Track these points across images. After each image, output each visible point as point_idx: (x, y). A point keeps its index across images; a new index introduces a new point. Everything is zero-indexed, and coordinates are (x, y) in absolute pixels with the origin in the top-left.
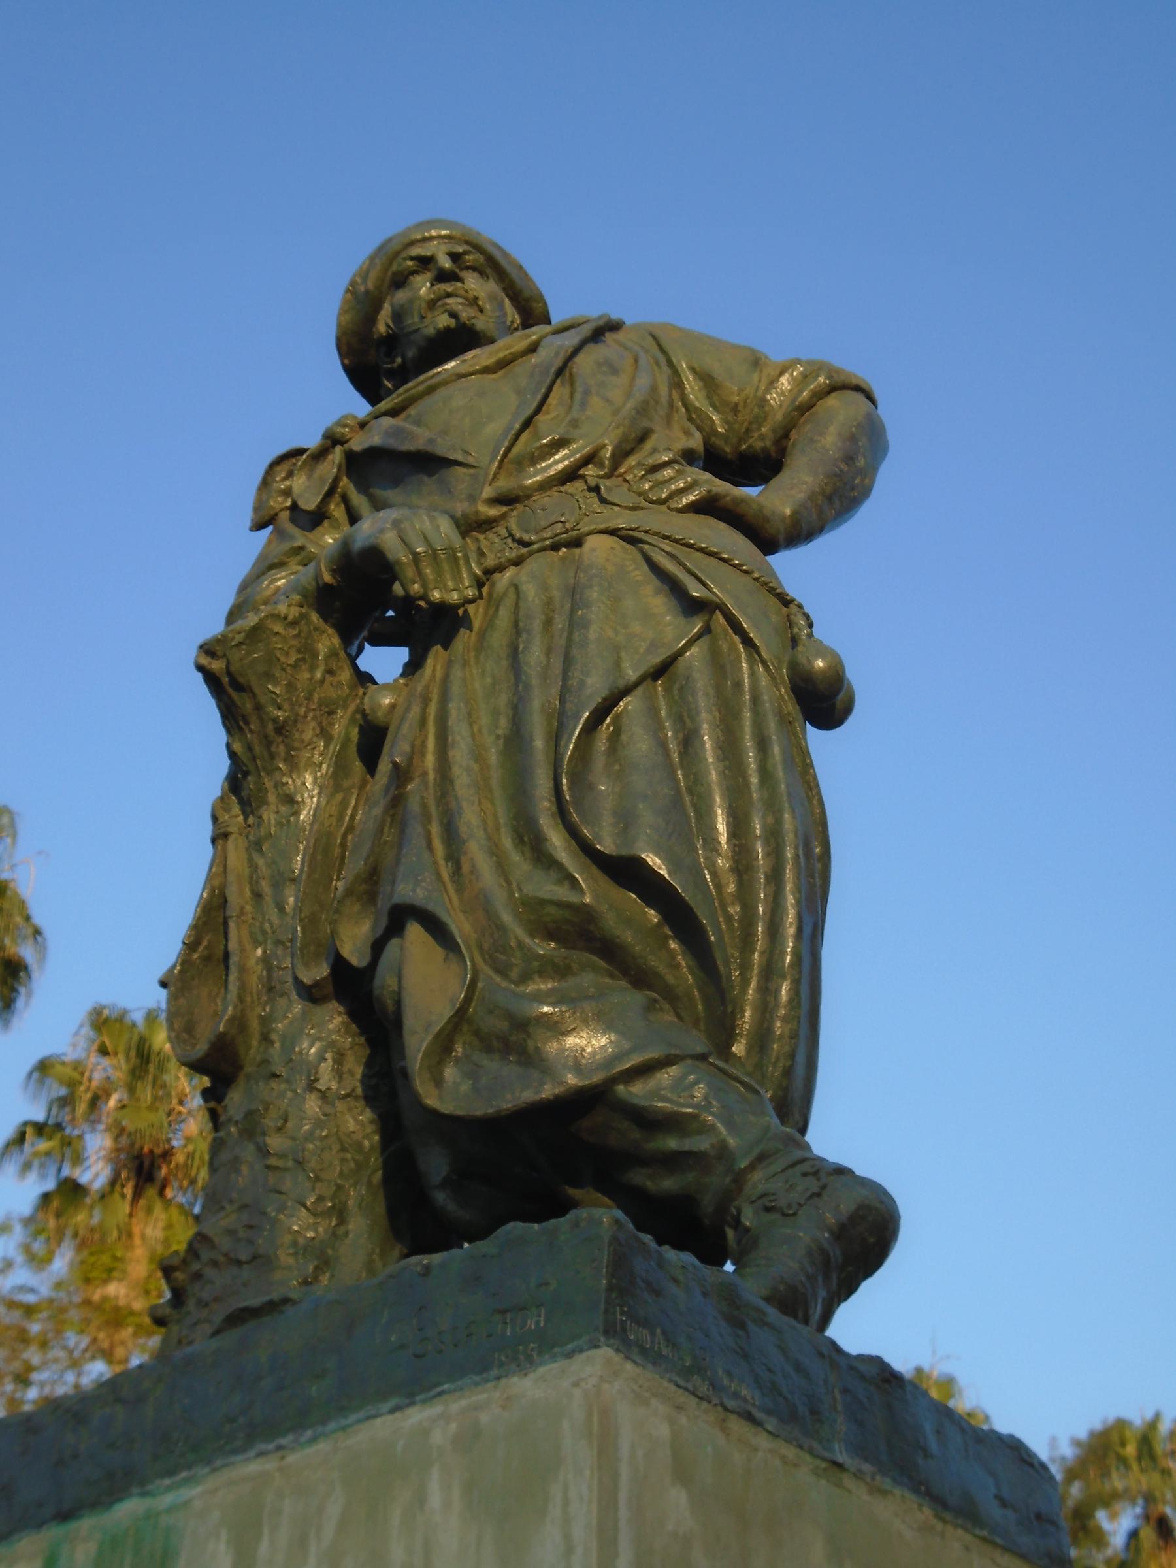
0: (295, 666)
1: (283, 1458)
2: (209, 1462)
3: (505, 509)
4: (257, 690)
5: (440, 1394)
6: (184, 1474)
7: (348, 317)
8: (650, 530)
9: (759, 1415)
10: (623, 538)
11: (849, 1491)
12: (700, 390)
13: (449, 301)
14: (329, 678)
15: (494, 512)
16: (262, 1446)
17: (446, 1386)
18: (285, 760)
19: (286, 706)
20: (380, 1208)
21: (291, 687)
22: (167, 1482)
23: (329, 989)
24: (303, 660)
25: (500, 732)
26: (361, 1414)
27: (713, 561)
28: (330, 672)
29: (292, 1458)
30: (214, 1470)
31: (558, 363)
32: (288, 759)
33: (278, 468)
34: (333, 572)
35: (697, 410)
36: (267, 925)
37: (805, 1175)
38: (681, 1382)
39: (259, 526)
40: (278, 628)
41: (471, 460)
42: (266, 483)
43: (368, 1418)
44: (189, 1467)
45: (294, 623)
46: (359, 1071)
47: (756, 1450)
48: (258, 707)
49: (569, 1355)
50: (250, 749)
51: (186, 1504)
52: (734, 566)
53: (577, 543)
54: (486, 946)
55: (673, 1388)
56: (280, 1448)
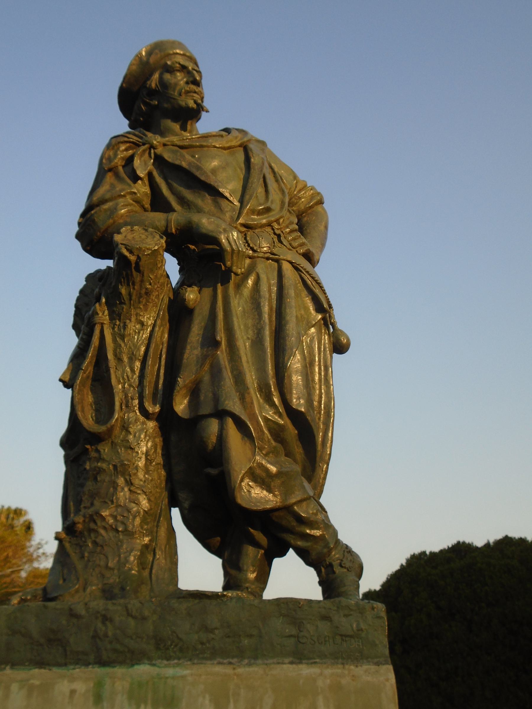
1: (234, 669)
2: (190, 660)
4: (145, 274)
6: (176, 661)
8: (303, 267)
10: (293, 266)
13: (195, 95)
17: (318, 660)
18: (144, 305)
22: (165, 662)
23: (155, 416)
26: (275, 660)
29: (240, 670)
30: (194, 664)
34: (177, 229)
36: (125, 377)
43: (279, 663)
44: (179, 659)
46: (160, 452)
48: (142, 281)
50: (130, 295)
51: (183, 677)
56: (230, 663)
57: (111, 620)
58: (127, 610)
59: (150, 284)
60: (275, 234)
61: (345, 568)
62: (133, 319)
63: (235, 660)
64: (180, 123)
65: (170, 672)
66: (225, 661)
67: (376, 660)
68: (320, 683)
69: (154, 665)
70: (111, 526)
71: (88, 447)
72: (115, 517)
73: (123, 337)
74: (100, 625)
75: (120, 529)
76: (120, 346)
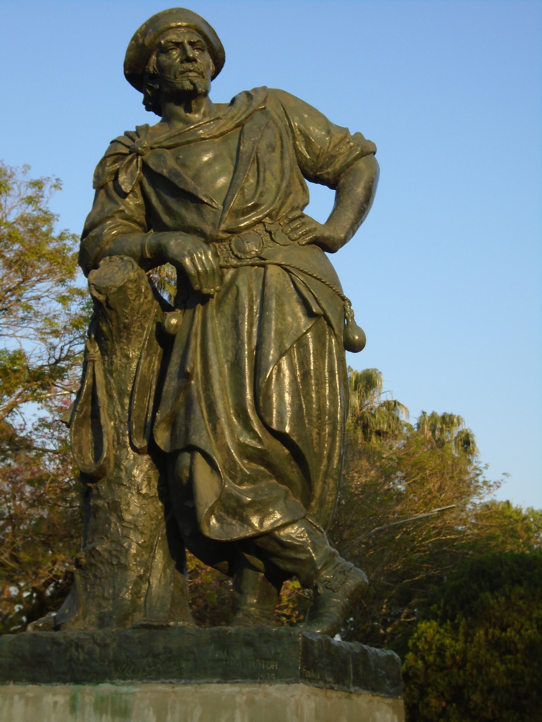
0: (134, 300)
1: (173, 687)
2: (140, 680)
3: (229, 235)
4: (118, 311)
5: (238, 682)
6: (130, 681)
7: (132, 53)
13: (191, 74)
15: (224, 236)
16: (164, 680)
17: (240, 680)
18: (126, 339)
19: (130, 318)
22: (122, 681)
23: (146, 450)
26: (205, 680)
27: (319, 282)
29: (178, 689)
30: (143, 683)
33: (108, 159)
34: (151, 254)
35: (300, 152)
36: (116, 414)
43: (208, 683)
44: (132, 679)
46: (156, 484)
48: (118, 317)
50: (110, 330)
51: (134, 694)
54: (227, 467)
56: (171, 683)
57: (82, 647)
58: (94, 639)
59: (127, 318)
60: (266, 231)
61: (330, 589)
62: (119, 354)
63: (174, 681)
64: (183, 105)
65: (125, 689)
66: (167, 681)
67: (288, 679)
68: (238, 699)
69: (113, 684)
70: (107, 560)
71: (90, 485)
72: (110, 552)
73: (111, 373)
74: (73, 650)
75: (114, 563)
76: (110, 382)
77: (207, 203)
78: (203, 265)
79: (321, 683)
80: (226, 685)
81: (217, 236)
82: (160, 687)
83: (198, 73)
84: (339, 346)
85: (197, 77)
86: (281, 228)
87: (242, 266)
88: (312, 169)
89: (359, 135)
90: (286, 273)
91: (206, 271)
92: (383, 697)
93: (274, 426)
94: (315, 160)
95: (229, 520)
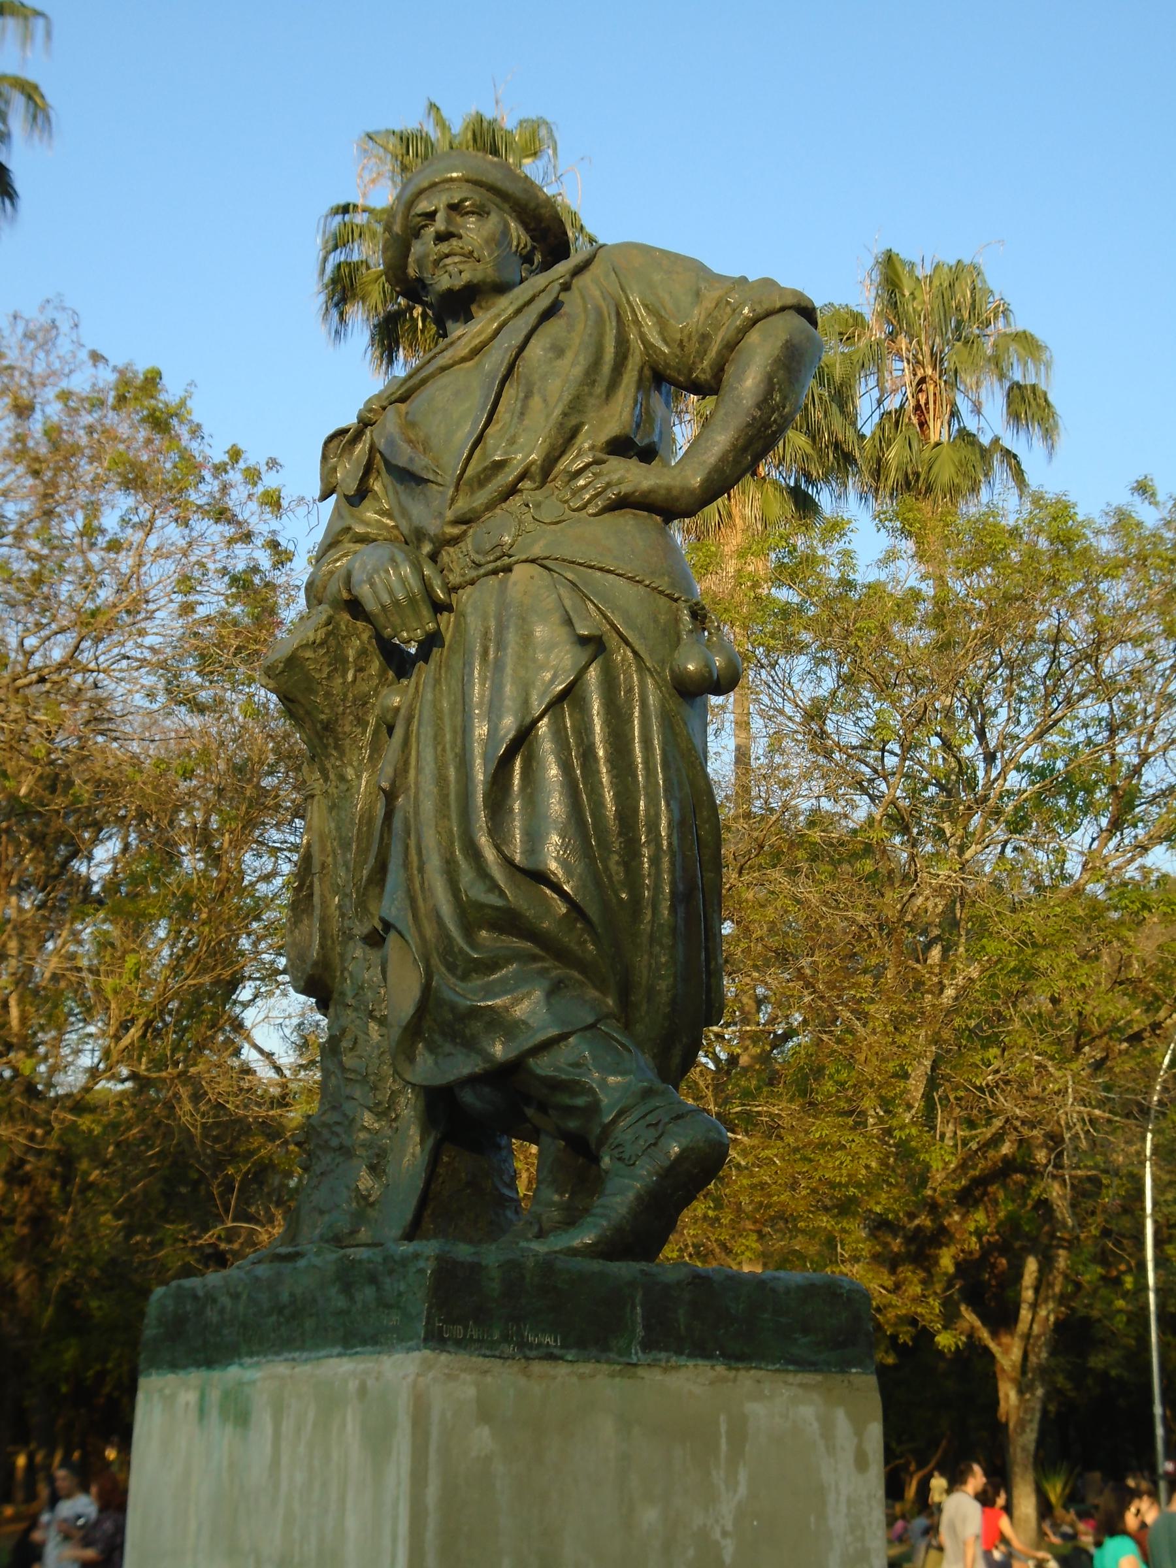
0: (329, 677)
3: (464, 527)
4: (303, 701)
5: (357, 1353)
7: (389, 254)
9: (557, 1352)
11: (643, 1378)
12: (654, 324)
13: (448, 261)
14: (360, 675)
15: (455, 531)
16: (286, 1355)
17: (358, 1349)
19: (327, 711)
20: (421, 1104)
21: (328, 695)
24: (336, 669)
25: (457, 750)
28: (360, 670)
30: (268, 1362)
31: (503, 370)
32: (336, 747)
35: (652, 345)
37: (649, 1126)
38: (488, 1353)
39: (324, 497)
40: (309, 654)
41: (439, 479)
42: (325, 458)
45: (322, 644)
47: (554, 1378)
49: (409, 1350)
51: (253, 1383)
52: (628, 578)
53: (508, 569)
55: (481, 1359)
56: (294, 1360)
59: (323, 713)
63: (296, 1355)
67: (410, 1344)
77: (428, 481)
78: (391, 593)
79: (509, 1350)
80: (345, 1359)
81: (444, 533)
82: (279, 1368)
83: (463, 255)
84: (660, 688)
85: (461, 262)
86: (557, 492)
87: (479, 578)
88: (679, 372)
89: (768, 283)
90: (546, 572)
91: (396, 603)
92: (777, 1371)
93: (518, 858)
94: (678, 351)
95: (448, 1047)
